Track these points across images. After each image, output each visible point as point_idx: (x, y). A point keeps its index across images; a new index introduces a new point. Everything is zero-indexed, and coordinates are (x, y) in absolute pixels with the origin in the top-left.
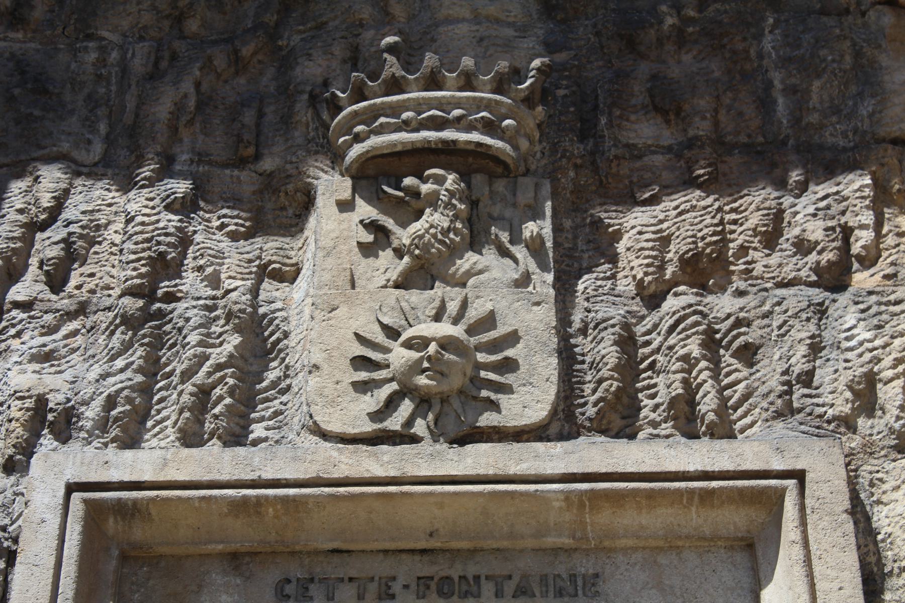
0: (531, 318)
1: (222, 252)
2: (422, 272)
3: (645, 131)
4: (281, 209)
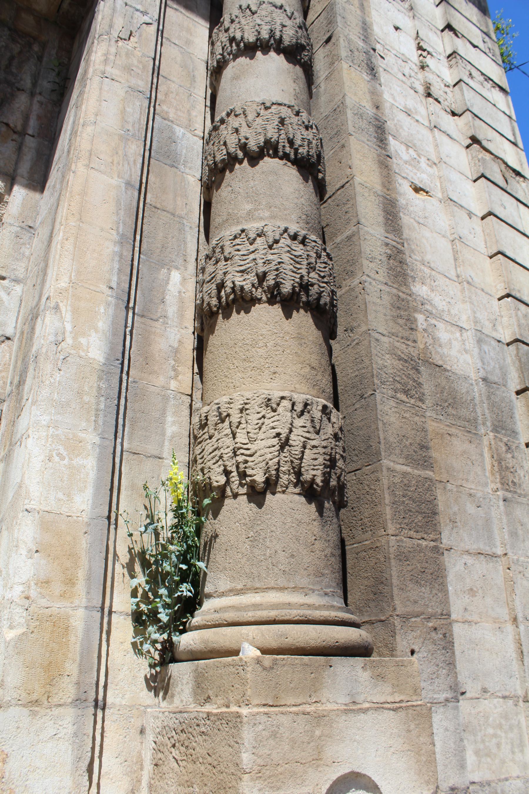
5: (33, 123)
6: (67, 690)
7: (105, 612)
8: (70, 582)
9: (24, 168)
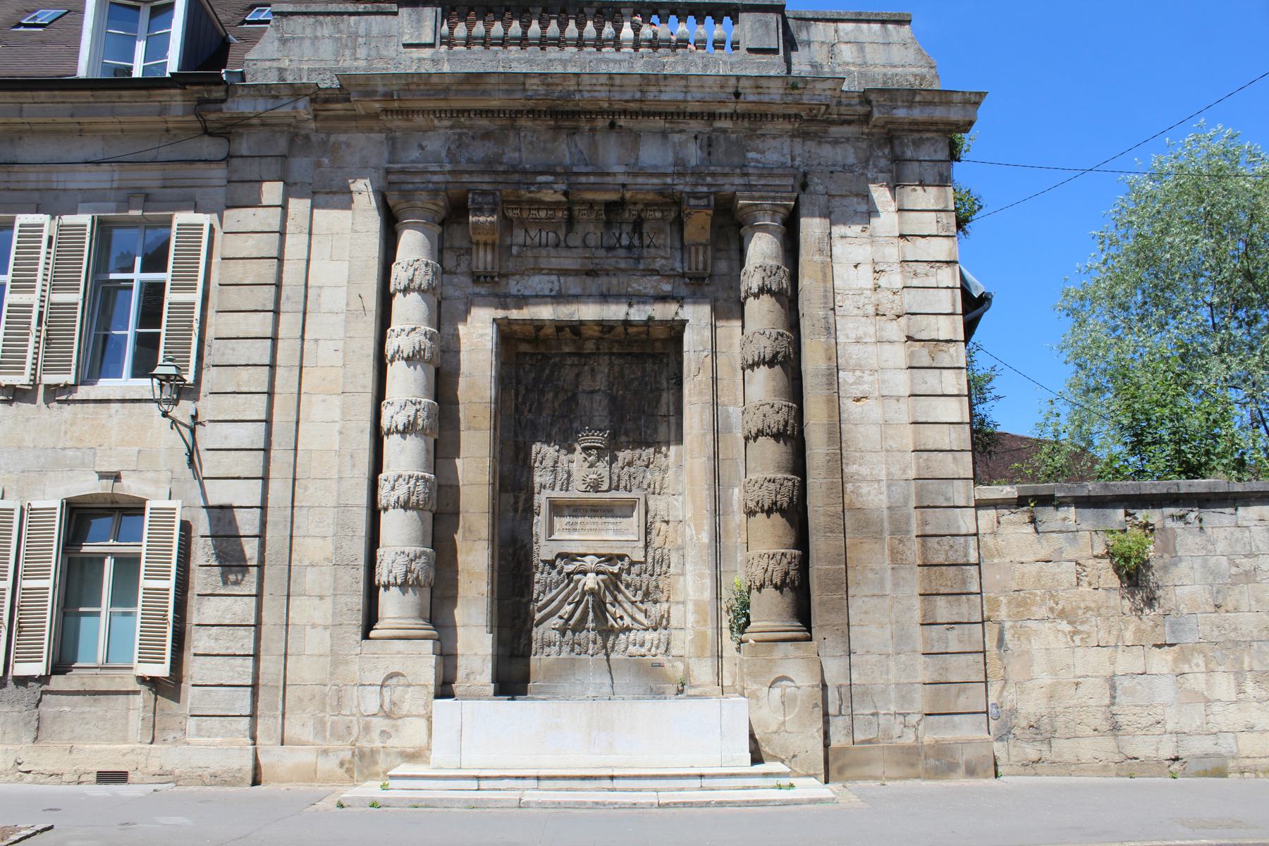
0: (606, 474)
1: (563, 458)
2: (591, 466)
3: (623, 439)
4: (571, 450)
5: (671, 408)
6: (708, 653)
7: (719, 630)
8: (706, 621)
9: (672, 437)
